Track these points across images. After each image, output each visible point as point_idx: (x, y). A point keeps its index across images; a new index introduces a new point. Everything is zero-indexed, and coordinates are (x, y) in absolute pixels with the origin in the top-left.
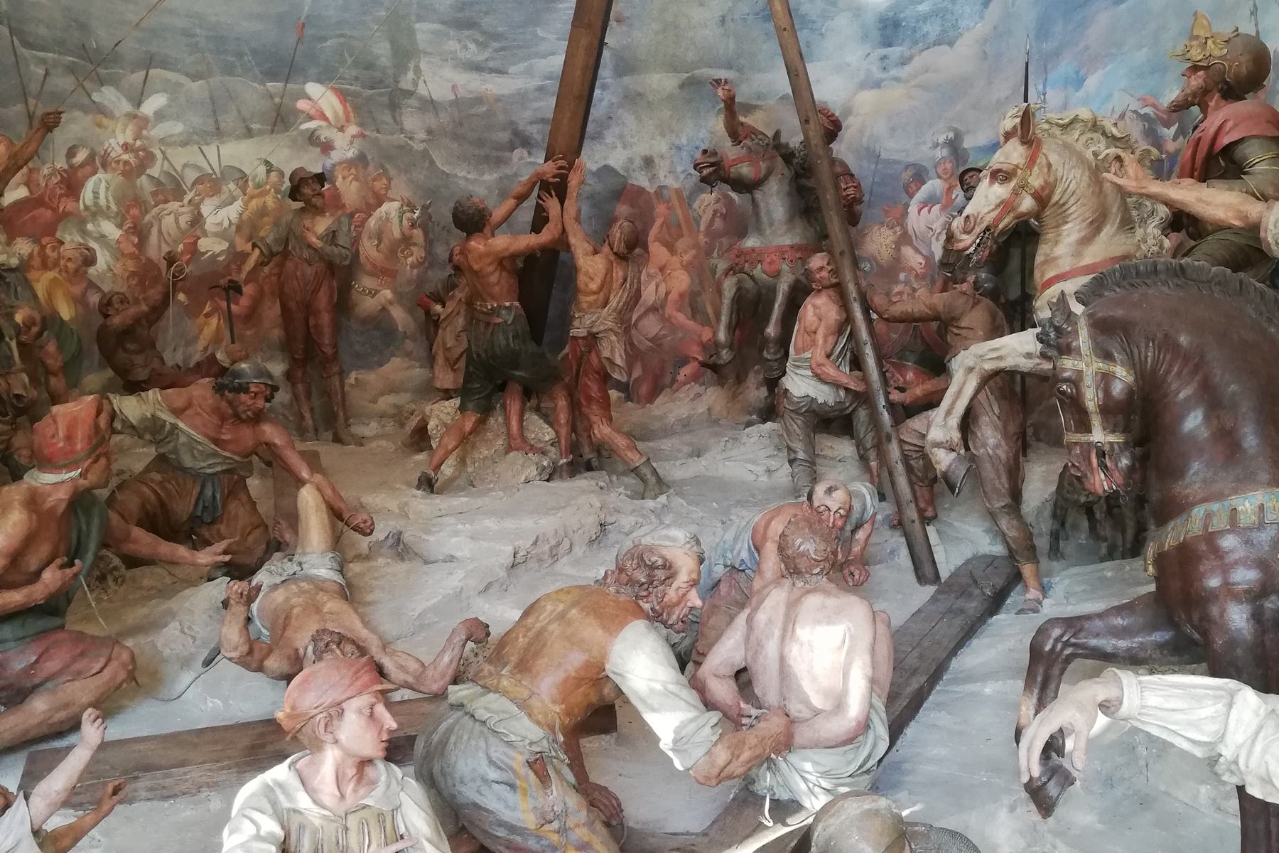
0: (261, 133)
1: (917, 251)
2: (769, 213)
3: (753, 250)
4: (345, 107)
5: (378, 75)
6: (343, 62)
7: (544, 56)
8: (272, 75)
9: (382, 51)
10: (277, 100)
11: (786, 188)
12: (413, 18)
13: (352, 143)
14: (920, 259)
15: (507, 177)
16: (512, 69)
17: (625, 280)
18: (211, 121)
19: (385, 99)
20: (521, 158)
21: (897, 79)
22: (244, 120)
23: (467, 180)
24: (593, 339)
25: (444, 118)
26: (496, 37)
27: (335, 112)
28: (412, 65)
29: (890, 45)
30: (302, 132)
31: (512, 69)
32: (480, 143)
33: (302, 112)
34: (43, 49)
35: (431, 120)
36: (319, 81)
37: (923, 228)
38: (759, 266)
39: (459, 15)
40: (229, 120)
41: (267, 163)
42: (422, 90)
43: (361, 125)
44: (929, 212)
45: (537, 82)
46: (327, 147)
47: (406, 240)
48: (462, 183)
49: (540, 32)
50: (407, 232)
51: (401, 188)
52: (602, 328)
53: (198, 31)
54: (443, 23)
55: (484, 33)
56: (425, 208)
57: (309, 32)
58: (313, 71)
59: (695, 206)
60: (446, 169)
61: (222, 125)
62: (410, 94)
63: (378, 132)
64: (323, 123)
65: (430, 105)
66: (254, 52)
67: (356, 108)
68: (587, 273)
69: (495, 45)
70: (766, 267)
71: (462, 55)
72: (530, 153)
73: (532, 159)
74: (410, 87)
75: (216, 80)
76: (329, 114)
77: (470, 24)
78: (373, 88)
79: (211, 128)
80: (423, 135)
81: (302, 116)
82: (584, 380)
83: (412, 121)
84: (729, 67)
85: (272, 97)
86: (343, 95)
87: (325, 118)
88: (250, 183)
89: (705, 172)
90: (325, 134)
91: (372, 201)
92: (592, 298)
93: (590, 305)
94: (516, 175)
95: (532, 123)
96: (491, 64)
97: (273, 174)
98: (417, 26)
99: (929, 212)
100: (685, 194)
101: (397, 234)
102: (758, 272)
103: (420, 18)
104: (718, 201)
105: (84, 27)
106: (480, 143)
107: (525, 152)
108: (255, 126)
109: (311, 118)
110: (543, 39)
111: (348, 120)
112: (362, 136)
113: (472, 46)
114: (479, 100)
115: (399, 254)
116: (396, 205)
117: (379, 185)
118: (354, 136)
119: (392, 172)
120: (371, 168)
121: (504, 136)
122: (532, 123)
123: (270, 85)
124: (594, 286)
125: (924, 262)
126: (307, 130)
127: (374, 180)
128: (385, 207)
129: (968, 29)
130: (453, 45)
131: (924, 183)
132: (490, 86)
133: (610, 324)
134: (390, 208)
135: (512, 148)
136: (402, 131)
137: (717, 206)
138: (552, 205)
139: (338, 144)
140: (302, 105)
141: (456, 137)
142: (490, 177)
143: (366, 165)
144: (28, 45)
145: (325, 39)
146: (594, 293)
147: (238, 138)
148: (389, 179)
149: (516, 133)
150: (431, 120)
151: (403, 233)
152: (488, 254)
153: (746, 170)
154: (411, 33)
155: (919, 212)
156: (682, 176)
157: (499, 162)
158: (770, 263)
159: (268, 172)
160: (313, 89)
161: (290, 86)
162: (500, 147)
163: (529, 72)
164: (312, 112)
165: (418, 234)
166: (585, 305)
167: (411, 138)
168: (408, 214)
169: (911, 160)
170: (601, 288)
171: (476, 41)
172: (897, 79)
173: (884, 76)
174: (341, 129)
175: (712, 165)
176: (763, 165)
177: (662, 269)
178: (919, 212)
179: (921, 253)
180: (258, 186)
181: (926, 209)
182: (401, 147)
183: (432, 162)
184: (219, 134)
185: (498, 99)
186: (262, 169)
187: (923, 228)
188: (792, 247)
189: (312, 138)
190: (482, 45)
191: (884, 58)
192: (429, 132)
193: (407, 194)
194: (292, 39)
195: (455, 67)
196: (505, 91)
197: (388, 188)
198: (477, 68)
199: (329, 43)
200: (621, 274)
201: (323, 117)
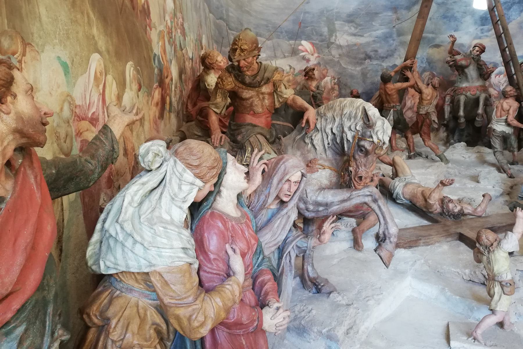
0: (288, 56)
1: (495, 89)
2: (471, 76)
3: (467, 87)
4: (314, 48)
5: (323, 37)
6: (313, 34)
7: (375, 31)
8: (291, 39)
9: (325, 30)
10: (293, 46)
11: (476, 68)
12: (334, 20)
13: (316, 59)
14: (496, 92)
15: (364, 68)
16: (365, 35)
17: (437, 96)
18: (273, 53)
19: (326, 45)
20: (368, 62)
21: (487, 36)
22: (283, 53)
23: (351, 69)
24: (427, 114)
25: (344, 50)
26: (360, 25)
27: (311, 50)
28: (334, 35)
29: (484, 25)
30: (300, 56)
31: (365, 35)
32: (355, 58)
33: (301, 50)
34: (233, 31)
35: (340, 51)
36: (305, 40)
37: (497, 82)
38: (469, 93)
39: (349, 19)
40: (279, 53)
41: (290, 66)
42: (337, 42)
43: (319, 53)
44: (499, 77)
45: (371, 39)
46: (308, 61)
47: (333, 89)
48: (350, 70)
49: (374, 23)
50: (333, 86)
51: (331, 72)
52: (431, 111)
53: (270, 25)
54: (344, 21)
55: (356, 24)
56: (338, 79)
57: (302, 25)
58: (303, 37)
59: (423, 76)
60: (345, 66)
61: (276, 54)
62: (333, 43)
63: (324, 55)
64: (307, 53)
65: (340, 47)
66: (286, 32)
67: (317, 48)
68: (426, 94)
69: (360, 28)
70: (472, 93)
71: (350, 31)
72: (371, 61)
73: (371, 63)
74: (334, 41)
75: (275, 40)
76: (309, 50)
77: (352, 22)
78: (322, 42)
79: (273, 55)
80: (338, 56)
81: (300, 51)
82: (424, 127)
83: (335, 52)
84: (433, 33)
85: (291, 45)
86: (313, 44)
87: (308, 52)
88: (285, 72)
89: (451, 63)
90: (308, 56)
91: (322, 77)
92: (428, 101)
93: (427, 104)
94: (367, 68)
95: (371, 51)
96: (359, 34)
97: (292, 69)
98: (336, 22)
99: (499, 77)
100: (420, 73)
101: (330, 87)
102: (468, 94)
103: (336, 20)
104: (430, 75)
105: (242, 24)
106: (355, 58)
107: (370, 61)
108: (286, 54)
109: (303, 52)
110: (375, 25)
111: (314, 52)
112: (319, 57)
113: (353, 28)
114: (355, 45)
115: (331, 93)
116: (330, 78)
117: (324, 72)
118: (316, 57)
119: (328, 68)
120: (322, 66)
121: (362, 56)
122: (371, 51)
123: (290, 42)
124: (429, 98)
125: (497, 93)
126: (302, 55)
127: (323, 70)
128: (326, 78)
129: (514, 19)
130: (346, 28)
131: (497, 68)
132: (358, 41)
133: (433, 110)
134: (328, 79)
135: (365, 59)
136: (331, 55)
137: (429, 76)
138: (409, 74)
139: (311, 59)
140: (300, 47)
141: (348, 56)
142: (359, 69)
143: (320, 66)
144: (230, 29)
145: (307, 27)
146: (429, 100)
147: (281, 58)
148: (327, 70)
149: (367, 55)
150: (340, 51)
151: (332, 87)
152: (394, 89)
153: (464, 63)
154: (334, 24)
155: (495, 77)
156: (419, 67)
157: (361, 64)
158: (473, 91)
159: (290, 68)
160: (304, 42)
161: (297, 42)
162: (362, 59)
163: (370, 36)
164: (303, 49)
165: (336, 87)
166: (425, 104)
167: (334, 57)
168: (333, 81)
169: (492, 61)
170: (430, 99)
171: (354, 27)
172: (487, 36)
173: (482, 35)
174: (312, 55)
175: (453, 61)
176: (469, 61)
177: (413, 96)
178: (495, 77)
179: (496, 90)
180: (287, 73)
181: (498, 76)
182: (331, 60)
183: (341, 65)
184: (275, 57)
185: (361, 44)
186: (288, 68)
187: (497, 82)
188: (480, 86)
189: (304, 58)
190: (356, 28)
191: (482, 30)
192: (340, 55)
193: (333, 74)
194: (297, 27)
195: (347, 35)
196: (363, 42)
197: (327, 73)
198: (354, 35)
199: (309, 28)
200: (436, 94)
201: (307, 51)
